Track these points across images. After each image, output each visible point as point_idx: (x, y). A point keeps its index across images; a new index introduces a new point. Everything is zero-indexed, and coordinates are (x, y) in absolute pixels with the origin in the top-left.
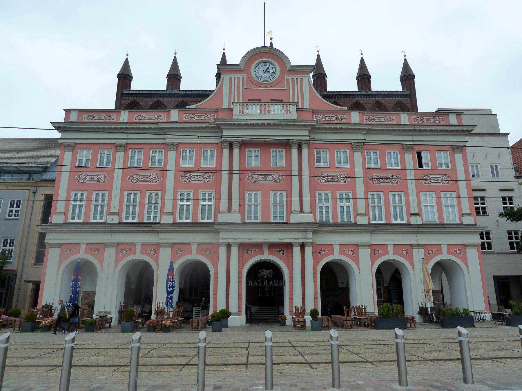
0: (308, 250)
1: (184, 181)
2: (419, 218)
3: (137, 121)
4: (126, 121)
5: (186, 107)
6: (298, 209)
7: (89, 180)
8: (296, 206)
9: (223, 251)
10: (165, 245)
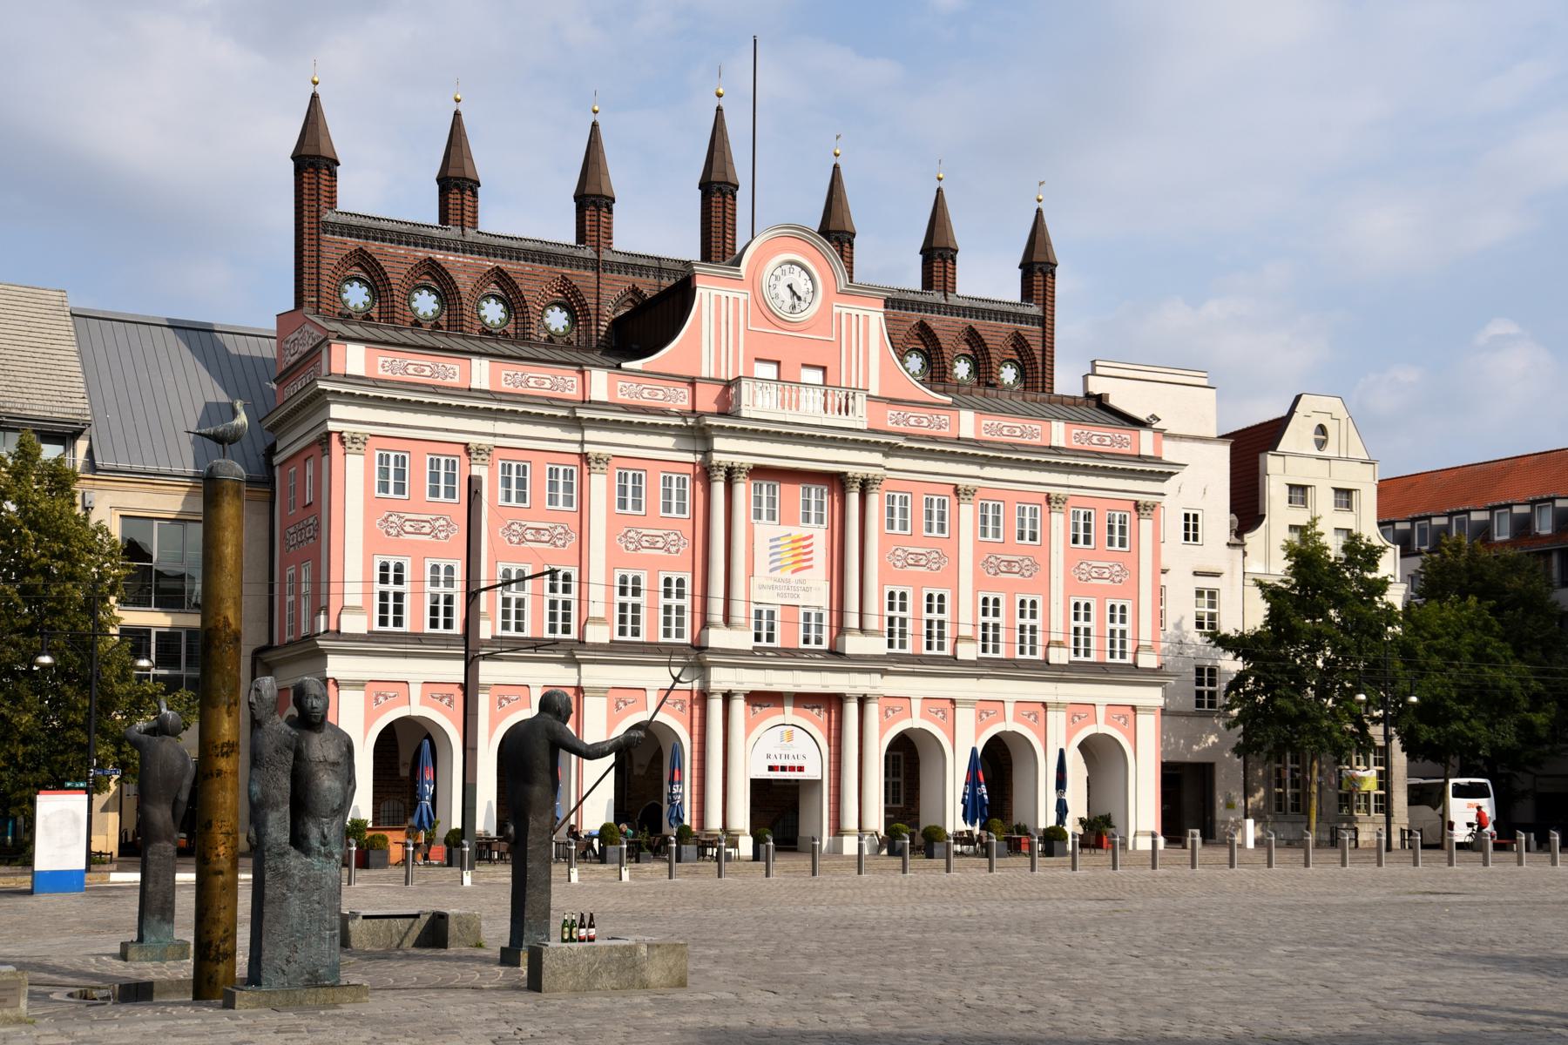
0: (873, 710)
5: (624, 365)
6: (857, 625)
9: (716, 705)
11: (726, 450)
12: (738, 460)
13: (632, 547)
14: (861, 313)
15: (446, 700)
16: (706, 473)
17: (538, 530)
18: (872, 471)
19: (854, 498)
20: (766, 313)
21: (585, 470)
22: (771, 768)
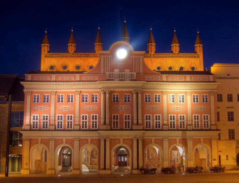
2: (191, 127)
5: (84, 73)
17: (65, 107)
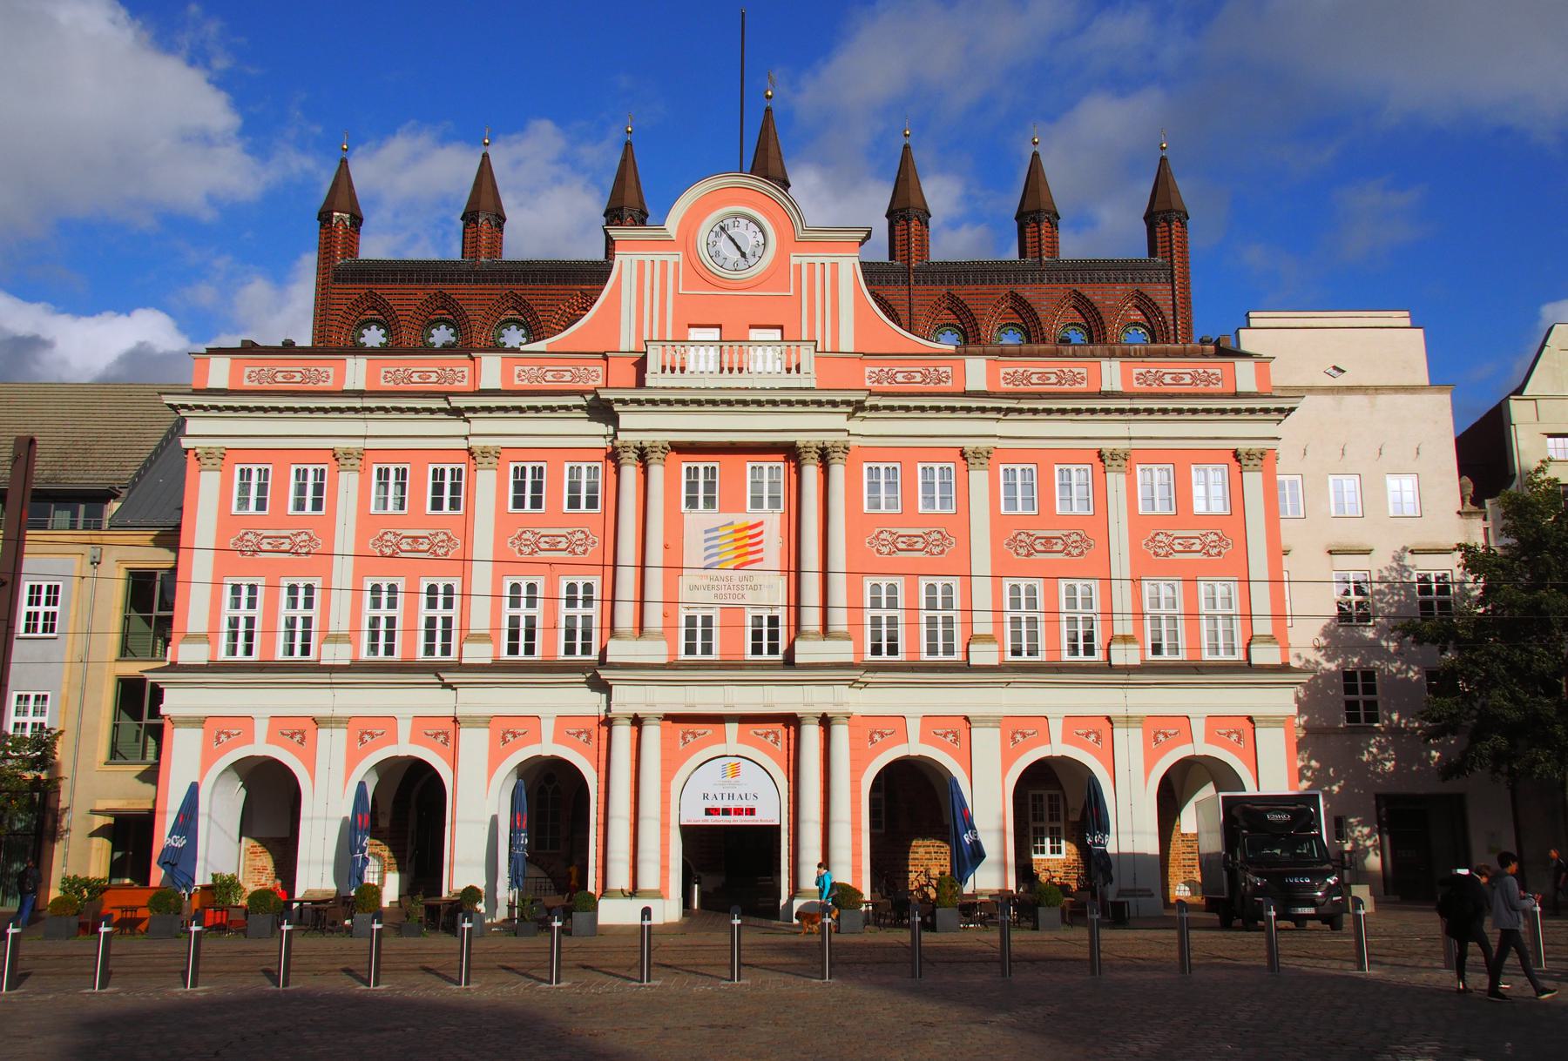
0: (841, 733)
1: (521, 551)
3: (391, 386)
4: (361, 386)
7: (269, 547)
8: (812, 619)
9: (623, 733)
10: (475, 722)
11: (637, 425)
12: (647, 438)
13: (526, 550)
14: (828, 261)
15: (298, 737)
16: (614, 456)
17: (415, 539)
18: (829, 438)
19: (811, 473)
20: (697, 271)
21: (472, 467)
22: (709, 812)
